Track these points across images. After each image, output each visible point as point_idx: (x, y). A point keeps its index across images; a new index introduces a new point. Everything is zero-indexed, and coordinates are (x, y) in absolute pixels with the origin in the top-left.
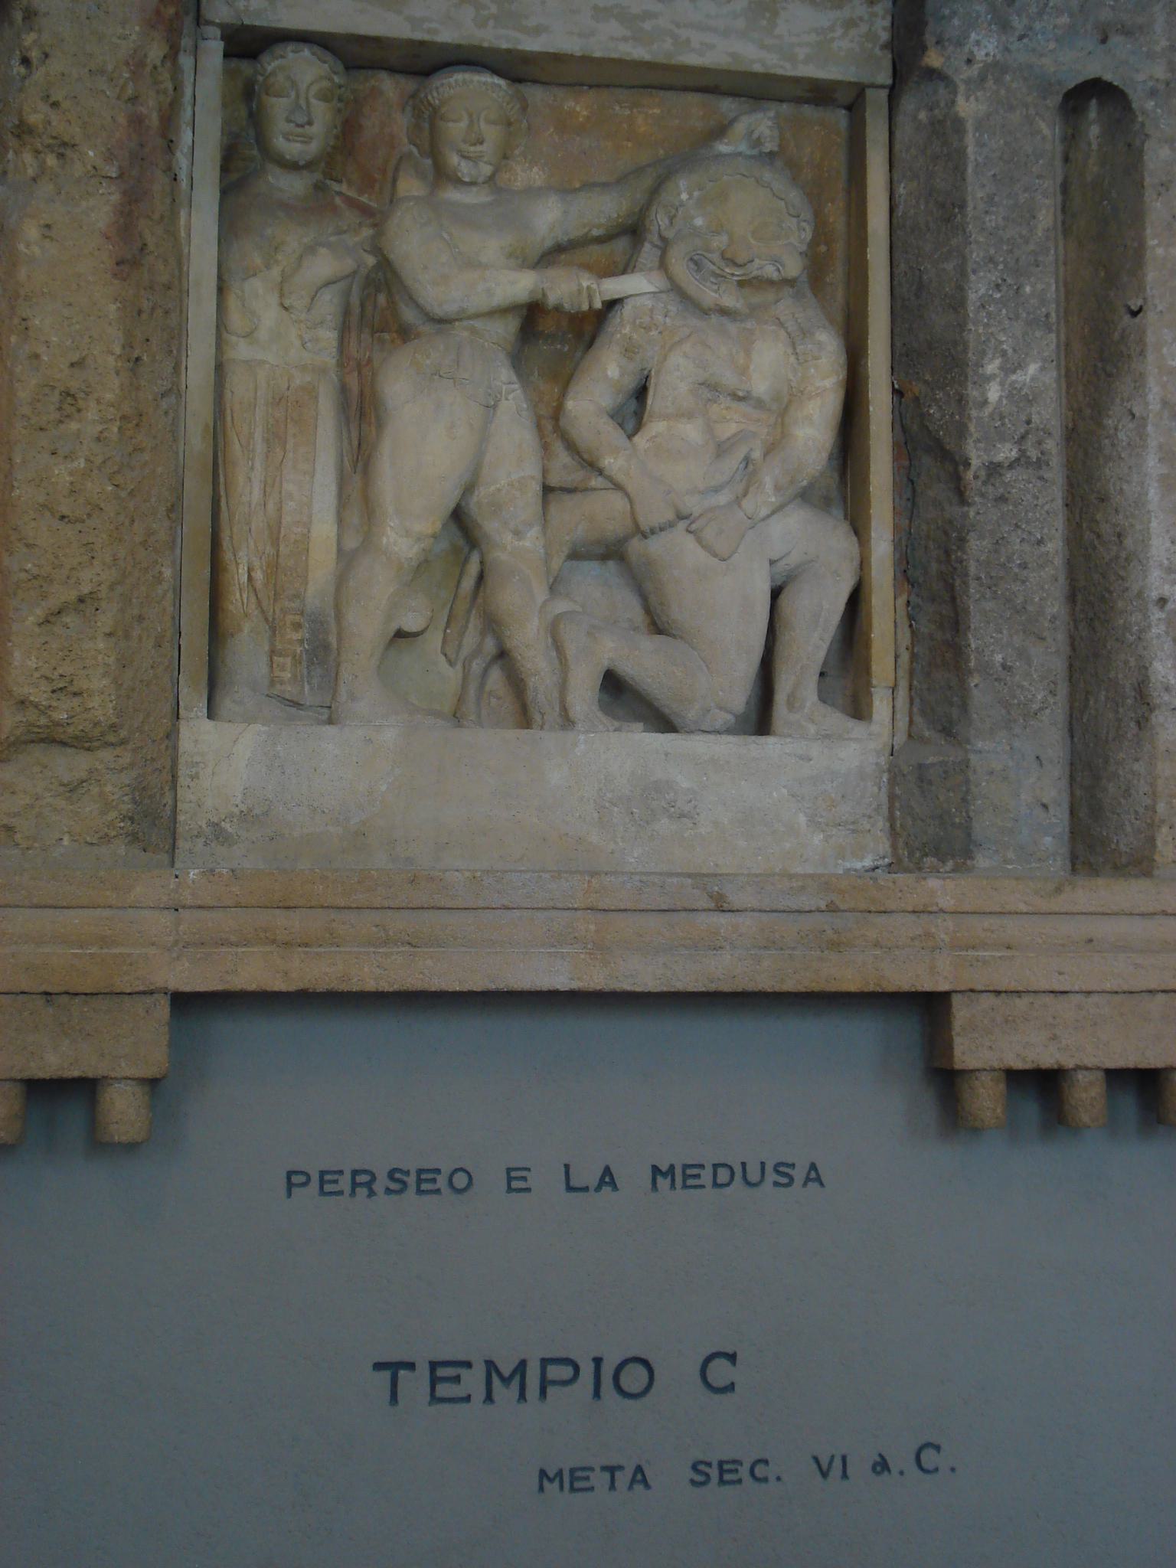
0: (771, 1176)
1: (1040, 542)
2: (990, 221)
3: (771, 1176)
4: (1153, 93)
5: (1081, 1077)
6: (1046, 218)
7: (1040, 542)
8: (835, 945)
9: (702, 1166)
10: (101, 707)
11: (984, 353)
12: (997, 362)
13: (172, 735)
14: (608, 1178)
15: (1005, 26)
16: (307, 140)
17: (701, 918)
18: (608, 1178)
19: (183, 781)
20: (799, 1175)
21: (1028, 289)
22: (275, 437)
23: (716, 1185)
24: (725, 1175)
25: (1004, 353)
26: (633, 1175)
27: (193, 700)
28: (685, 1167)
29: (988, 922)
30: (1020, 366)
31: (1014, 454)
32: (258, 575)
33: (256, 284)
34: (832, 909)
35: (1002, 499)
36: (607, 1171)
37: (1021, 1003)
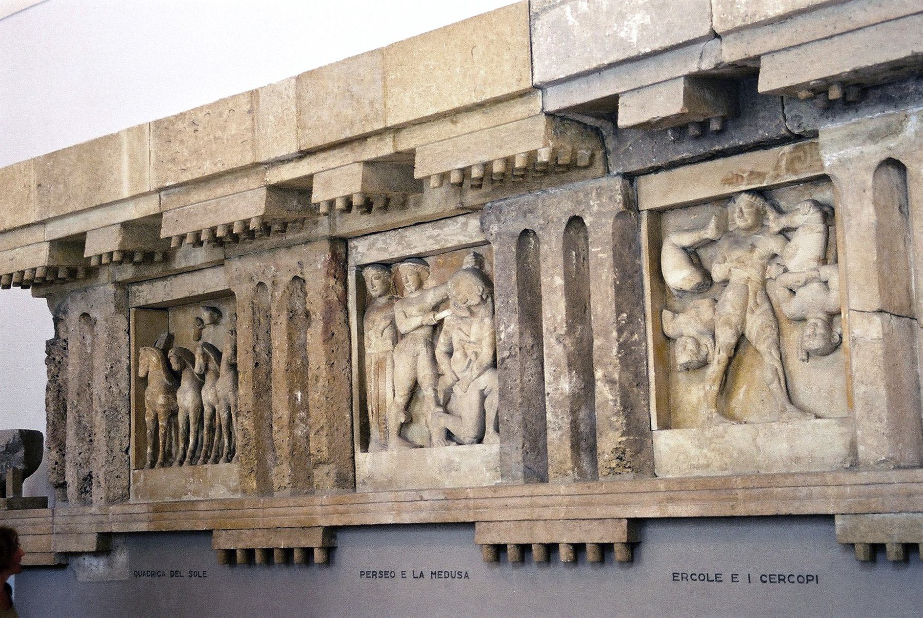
0: (457, 575)
1: (515, 380)
2: (501, 282)
3: (457, 575)
4: (541, 228)
5: (509, 547)
6: (514, 278)
7: (515, 380)
8: (447, 509)
9: (678, 574)
10: (325, 454)
11: (499, 324)
12: (503, 326)
13: (353, 457)
14: (422, 575)
15: (499, 220)
16: (376, 291)
17: (419, 502)
18: (422, 575)
19: (357, 469)
20: (463, 575)
21: (510, 301)
22: (377, 374)
23: (445, 577)
24: (448, 574)
25: (505, 323)
26: (427, 575)
27: (357, 447)
28: (439, 572)
29: (482, 501)
30: (509, 326)
31: (508, 354)
32: (374, 411)
33: (371, 332)
34: (446, 499)
35: (506, 368)
36: (422, 573)
37: (491, 524)
